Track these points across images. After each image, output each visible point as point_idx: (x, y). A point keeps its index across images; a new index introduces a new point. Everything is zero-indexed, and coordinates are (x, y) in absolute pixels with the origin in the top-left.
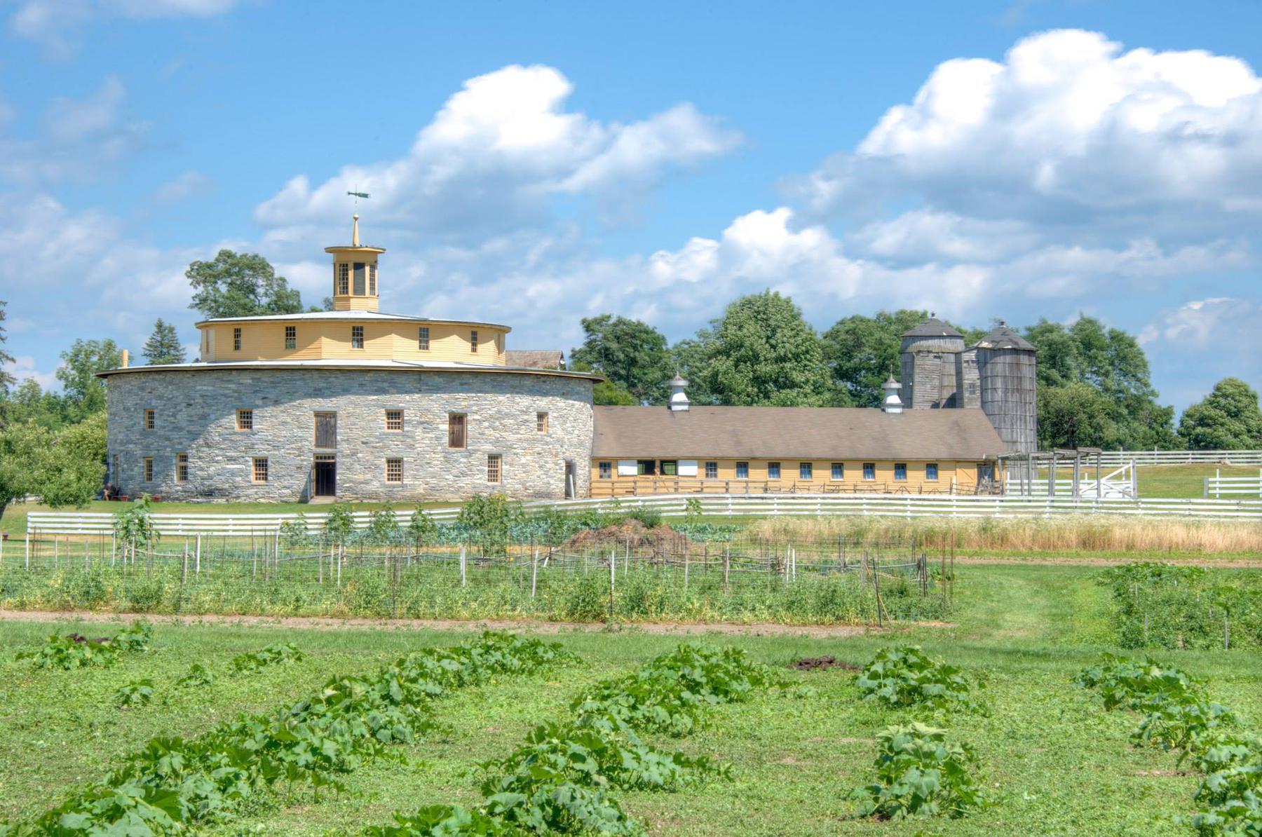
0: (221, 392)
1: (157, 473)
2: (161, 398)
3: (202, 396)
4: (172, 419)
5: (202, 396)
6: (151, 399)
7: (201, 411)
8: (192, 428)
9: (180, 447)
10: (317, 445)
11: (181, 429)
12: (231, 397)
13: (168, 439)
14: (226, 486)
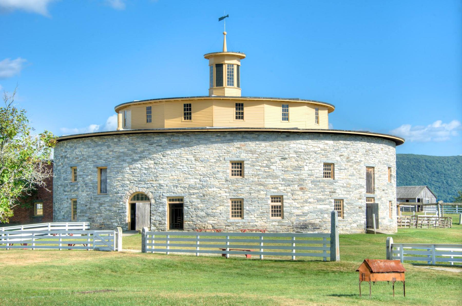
0: (313, 149)
1: (249, 212)
2: (252, 152)
3: (296, 152)
4: (267, 169)
5: (296, 152)
6: (240, 153)
7: (296, 164)
8: (287, 176)
9: (276, 191)
10: (367, 192)
11: (277, 177)
12: (319, 153)
13: (260, 185)
14: (317, 221)
